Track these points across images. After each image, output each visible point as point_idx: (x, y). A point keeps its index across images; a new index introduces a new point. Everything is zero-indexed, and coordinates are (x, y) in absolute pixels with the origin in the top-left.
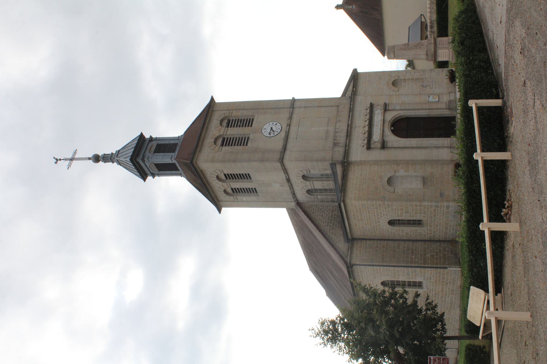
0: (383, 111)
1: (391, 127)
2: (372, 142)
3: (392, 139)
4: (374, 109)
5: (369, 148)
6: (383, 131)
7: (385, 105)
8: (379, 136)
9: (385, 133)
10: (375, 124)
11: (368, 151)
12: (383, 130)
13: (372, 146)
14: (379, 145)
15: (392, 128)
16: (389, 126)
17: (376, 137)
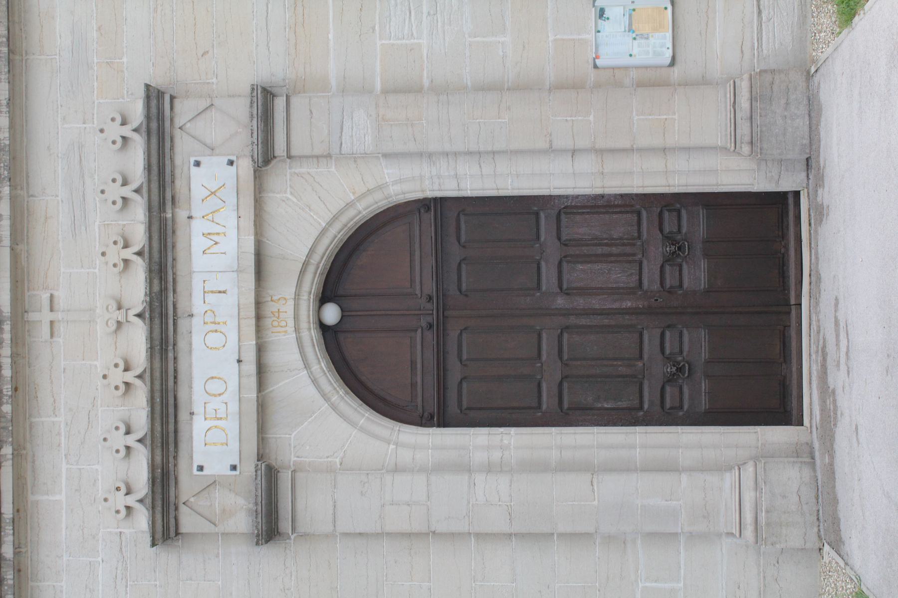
0: (246, 166)
1: (324, 299)
2: (187, 485)
3: (328, 426)
4: (184, 148)
5: (166, 529)
6: (261, 370)
7: (265, 100)
8: (232, 426)
9: (279, 386)
10: (198, 305)
11: (166, 556)
12: (260, 349)
13: (188, 521)
14: (239, 512)
15: (331, 314)
16: (312, 284)
17: (214, 439)
